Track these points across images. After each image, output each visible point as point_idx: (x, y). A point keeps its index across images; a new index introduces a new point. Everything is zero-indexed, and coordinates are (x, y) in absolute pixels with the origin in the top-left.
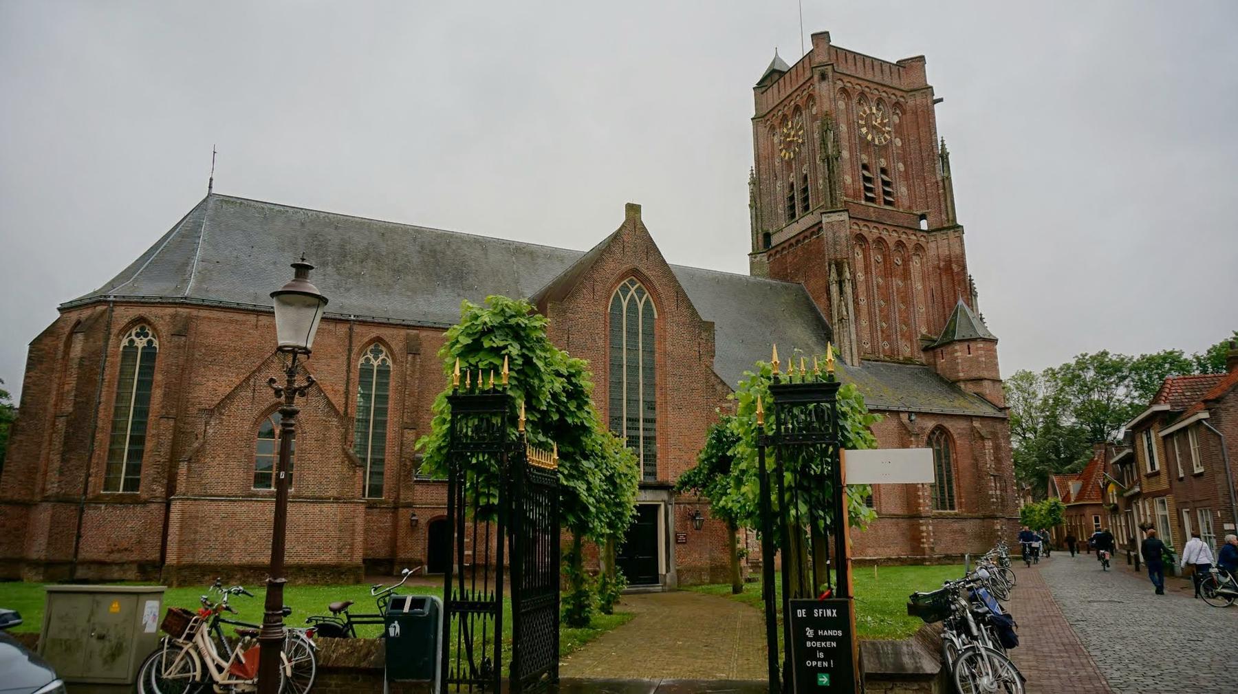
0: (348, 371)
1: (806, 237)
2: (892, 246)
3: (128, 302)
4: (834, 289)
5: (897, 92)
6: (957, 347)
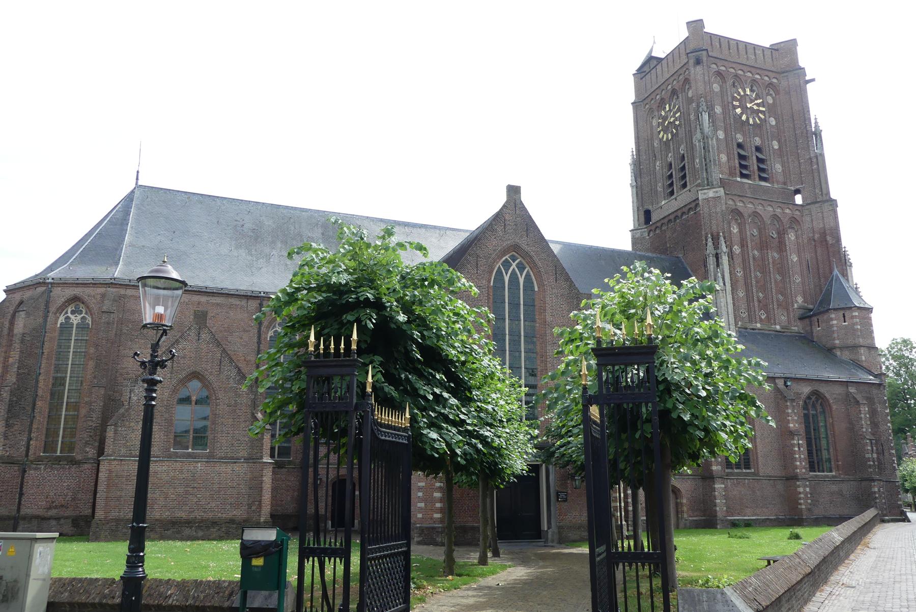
0: (259, 343)
1: (683, 213)
3: (63, 283)
4: (711, 261)
5: (770, 74)
6: (833, 316)
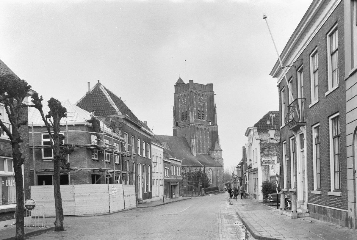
2: (203, 129)
